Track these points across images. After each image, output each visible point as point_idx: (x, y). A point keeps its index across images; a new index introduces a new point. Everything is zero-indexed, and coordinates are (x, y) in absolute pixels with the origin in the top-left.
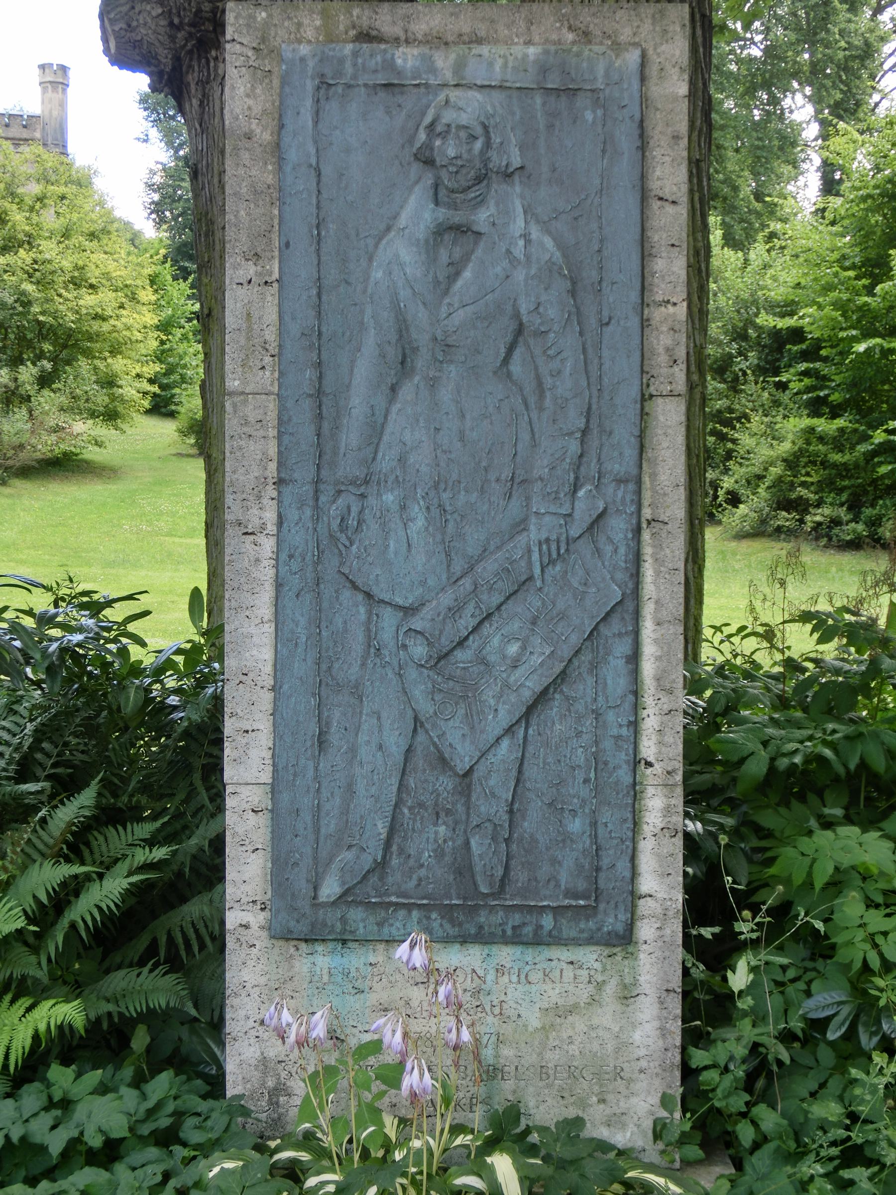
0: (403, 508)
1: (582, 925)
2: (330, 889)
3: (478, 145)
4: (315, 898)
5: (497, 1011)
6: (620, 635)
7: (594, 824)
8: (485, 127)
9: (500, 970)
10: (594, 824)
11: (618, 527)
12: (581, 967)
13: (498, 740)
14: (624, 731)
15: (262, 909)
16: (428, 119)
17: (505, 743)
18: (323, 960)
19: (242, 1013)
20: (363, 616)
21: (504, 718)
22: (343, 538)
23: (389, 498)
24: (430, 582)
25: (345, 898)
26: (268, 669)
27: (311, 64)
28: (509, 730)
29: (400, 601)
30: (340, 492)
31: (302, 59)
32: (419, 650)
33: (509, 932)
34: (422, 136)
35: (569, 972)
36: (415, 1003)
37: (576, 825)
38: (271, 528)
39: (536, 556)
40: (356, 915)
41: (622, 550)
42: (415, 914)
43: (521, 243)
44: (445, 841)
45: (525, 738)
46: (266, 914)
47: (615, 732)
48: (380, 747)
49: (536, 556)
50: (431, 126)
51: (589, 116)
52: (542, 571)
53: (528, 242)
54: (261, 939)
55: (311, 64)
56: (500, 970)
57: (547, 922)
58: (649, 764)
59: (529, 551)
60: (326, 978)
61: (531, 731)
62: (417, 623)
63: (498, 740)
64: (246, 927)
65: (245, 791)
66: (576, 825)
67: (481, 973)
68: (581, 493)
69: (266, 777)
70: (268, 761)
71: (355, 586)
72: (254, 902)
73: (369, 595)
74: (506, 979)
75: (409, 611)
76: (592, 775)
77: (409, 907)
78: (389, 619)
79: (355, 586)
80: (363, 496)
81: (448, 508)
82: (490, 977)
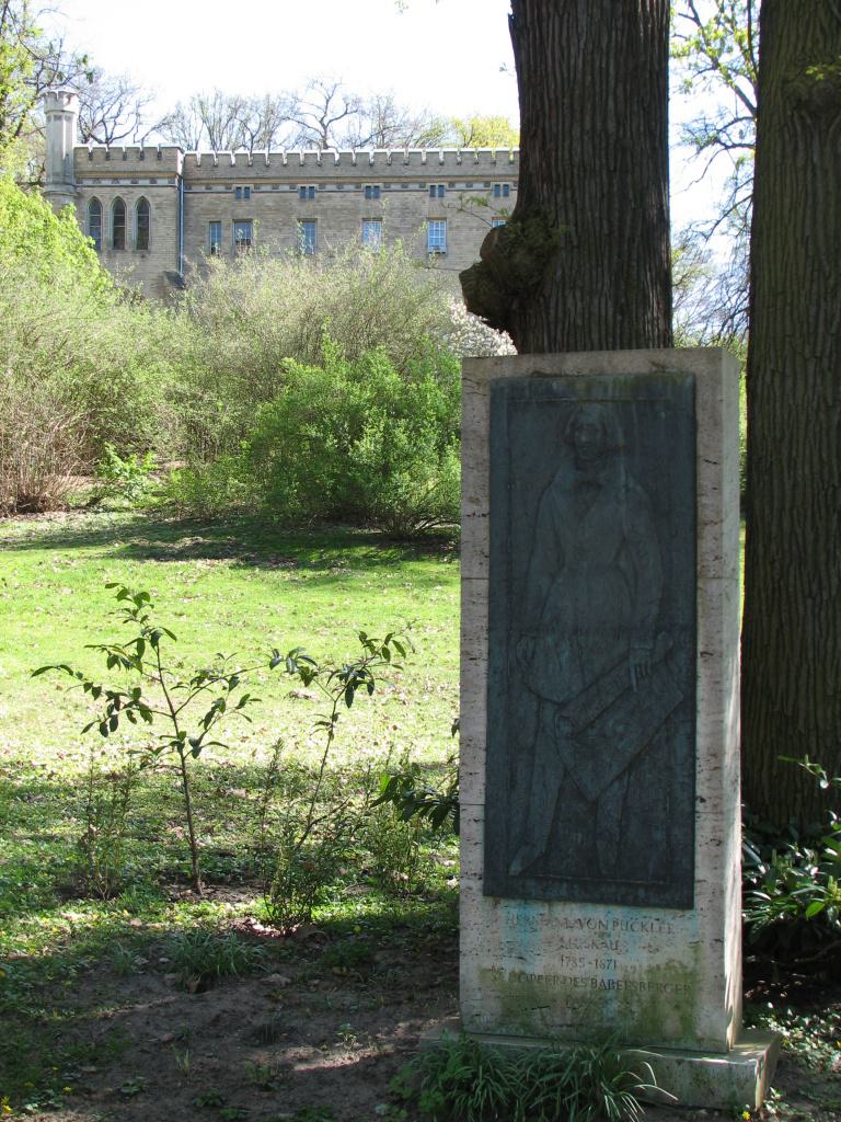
0: (557, 645)
1: (662, 897)
2: (515, 868)
3: (599, 436)
4: (508, 872)
5: (614, 947)
6: (684, 721)
7: (668, 835)
8: (603, 425)
9: (615, 923)
10: (668, 835)
11: (682, 657)
12: (663, 923)
13: (612, 783)
14: (687, 780)
15: (480, 879)
16: (572, 419)
17: (616, 785)
18: (510, 910)
19: (468, 940)
20: (535, 708)
21: (616, 770)
22: (524, 663)
23: (550, 640)
24: (574, 689)
25: (523, 874)
26: (483, 737)
27: (506, 391)
28: (619, 778)
29: (555, 699)
30: (522, 636)
31: (502, 389)
32: (566, 729)
33: (619, 899)
34: (568, 430)
35: (656, 926)
36: (566, 939)
37: (659, 836)
38: (485, 656)
39: (633, 675)
40: (531, 883)
41: (684, 670)
42: (565, 885)
43: (623, 490)
44: (582, 842)
45: (628, 782)
46: (481, 882)
47: (681, 780)
48: (544, 785)
49: (633, 675)
50: (573, 425)
51: (663, 415)
52: (637, 683)
53: (628, 490)
54: (480, 898)
55: (506, 391)
56: (615, 923)
57: (641, 893)
58: (703, 800)
59: (629, 670)
60: (515, 922)
61: (632, 778)
62: (565, 714)
63: (612, 783)
64: (470, 889)
65: (470, 809)
66: (659, 836)
67: (604, 923)
68: (660, 637)
69: (482, 801)
70: (483, 791)
71: (530, 690)
72: (475, 874)
73: (539, 696)
74: (619, 927)
75: (561, 706)
76: (668, 805)
77: (561, 881)
78: (549, 713)
79: (530, 690)
80: (534, 638)
81: (584, 645)
82: (610, 926)
